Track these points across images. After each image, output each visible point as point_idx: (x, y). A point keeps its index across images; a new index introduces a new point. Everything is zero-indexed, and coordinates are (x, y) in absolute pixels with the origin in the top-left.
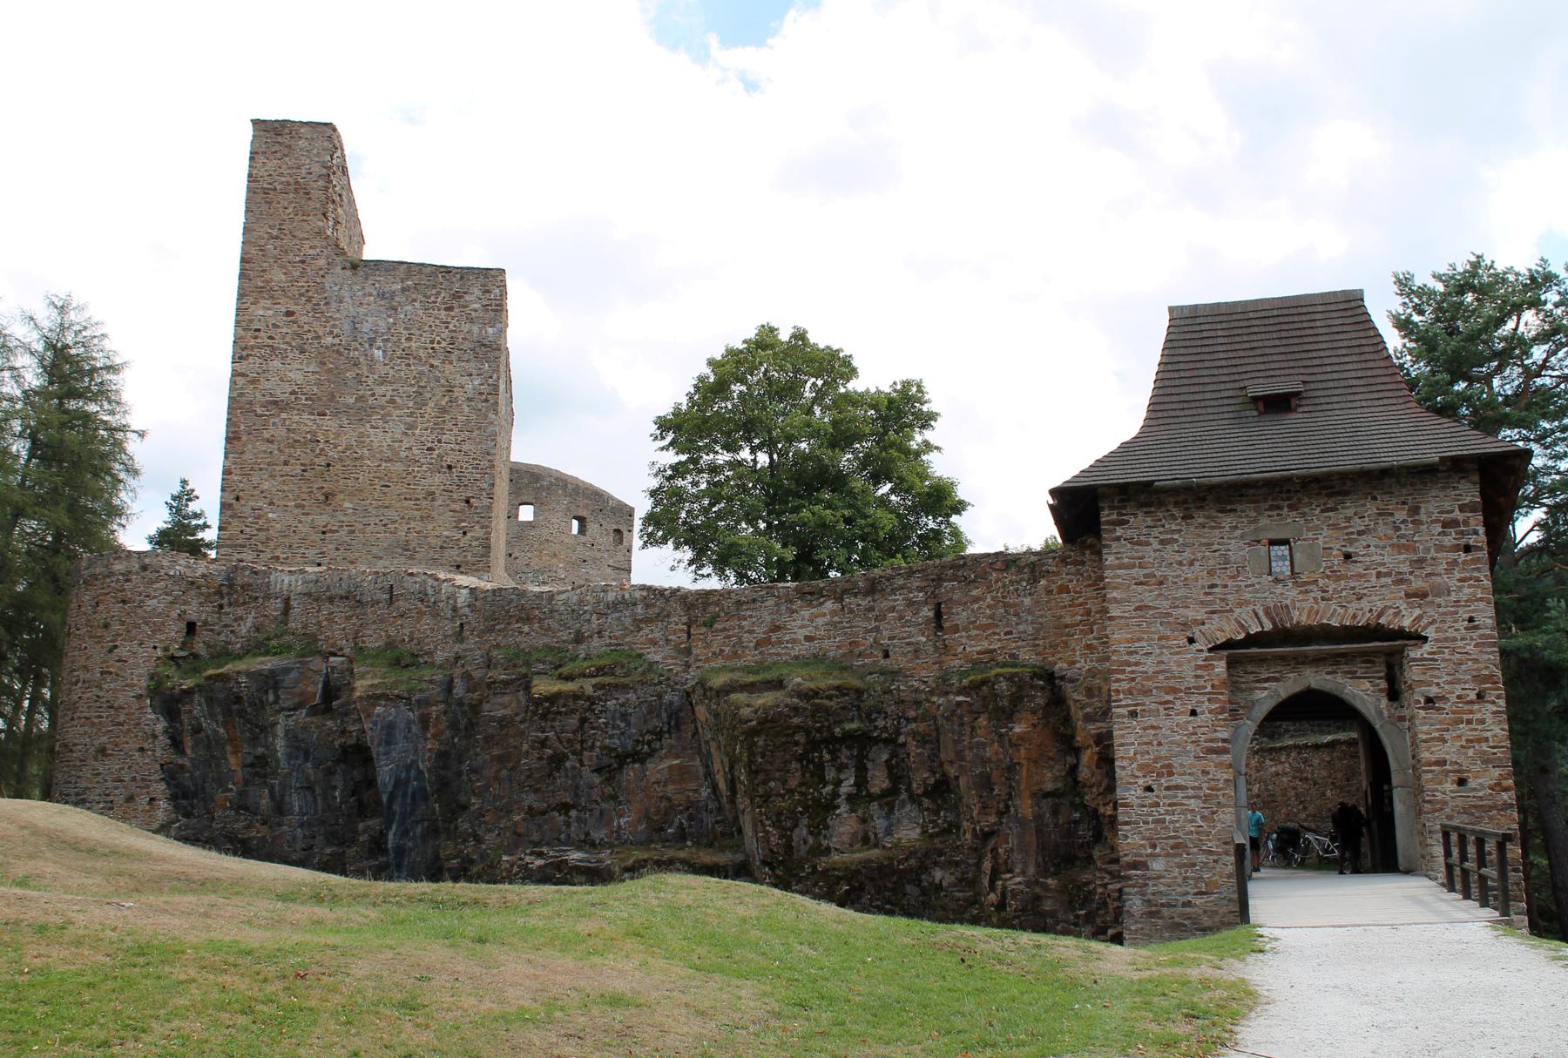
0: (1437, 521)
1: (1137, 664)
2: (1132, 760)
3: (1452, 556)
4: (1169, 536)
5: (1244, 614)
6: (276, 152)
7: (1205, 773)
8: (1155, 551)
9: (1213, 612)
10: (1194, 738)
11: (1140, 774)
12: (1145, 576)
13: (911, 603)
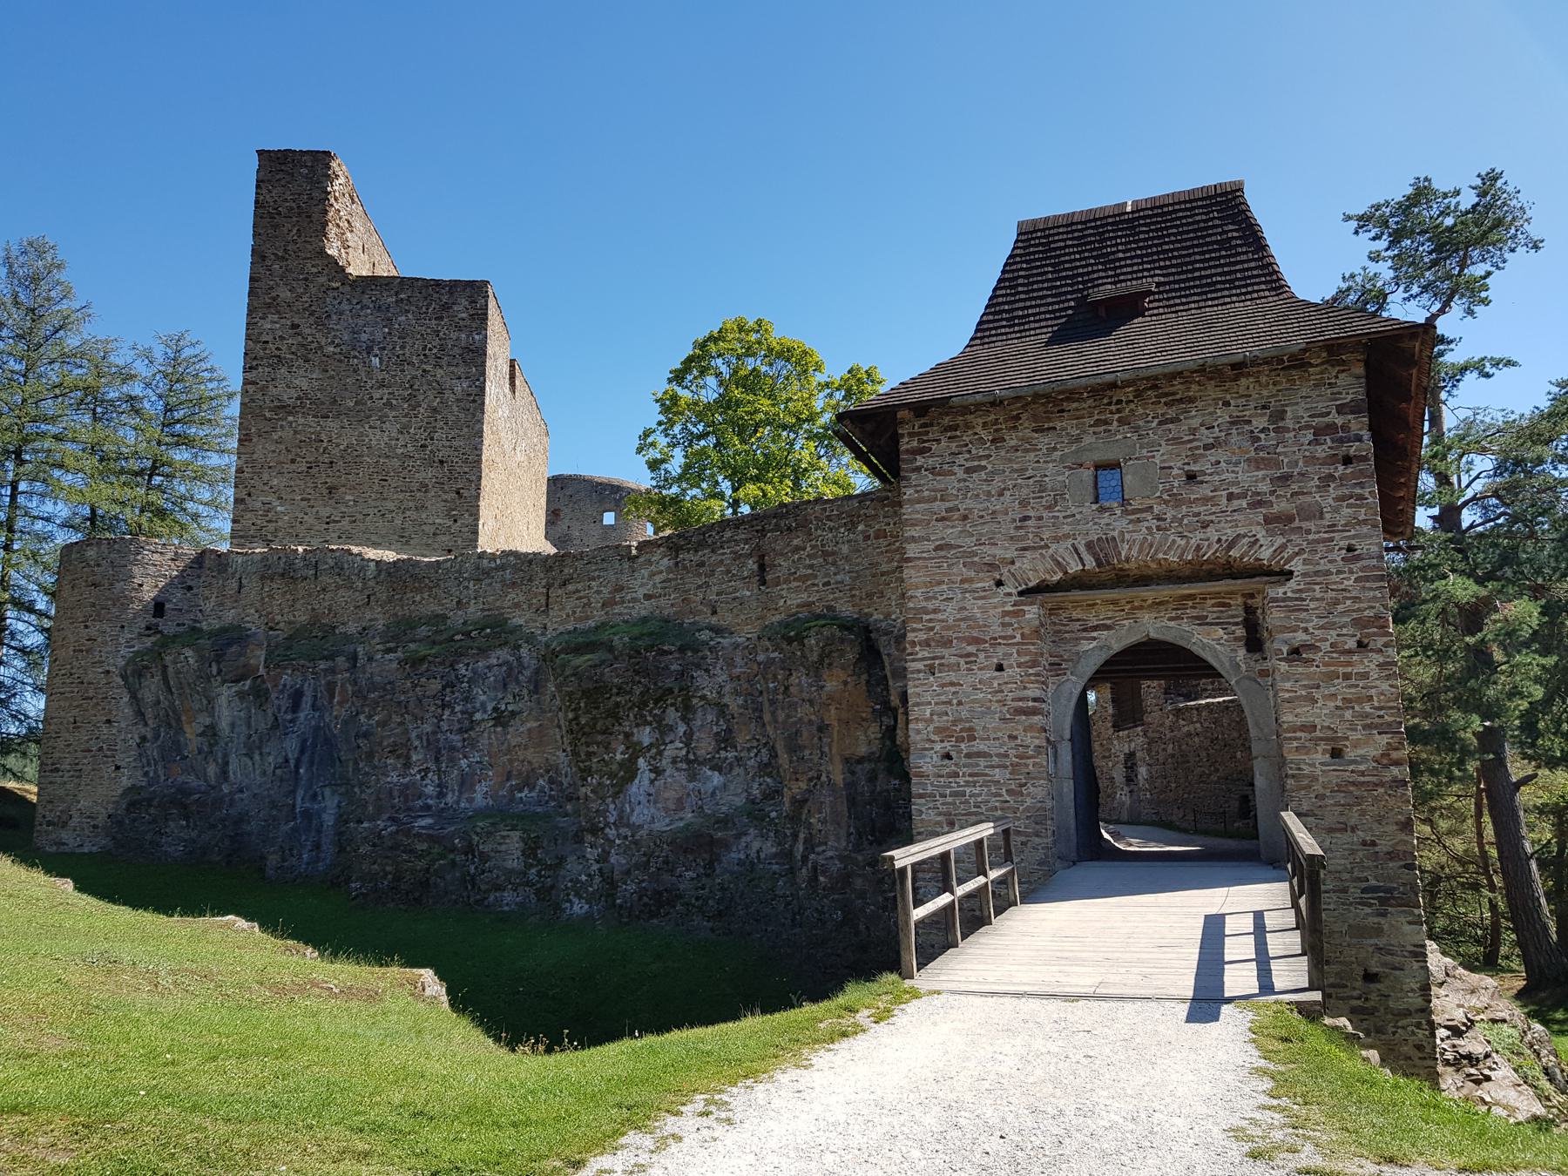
0: (1308, 427)
1: (935, 611)
2: (930, 721)
3: (1326, 470)
4: (976, 463)
5: (1062, 550)
6: (279, 180)
7: (1013, 737)
8: (959, 481)
9: (1025, 549)
10: (999, 696)
11: (936, 738)
12: (948, 510)
13: (737, 556)
